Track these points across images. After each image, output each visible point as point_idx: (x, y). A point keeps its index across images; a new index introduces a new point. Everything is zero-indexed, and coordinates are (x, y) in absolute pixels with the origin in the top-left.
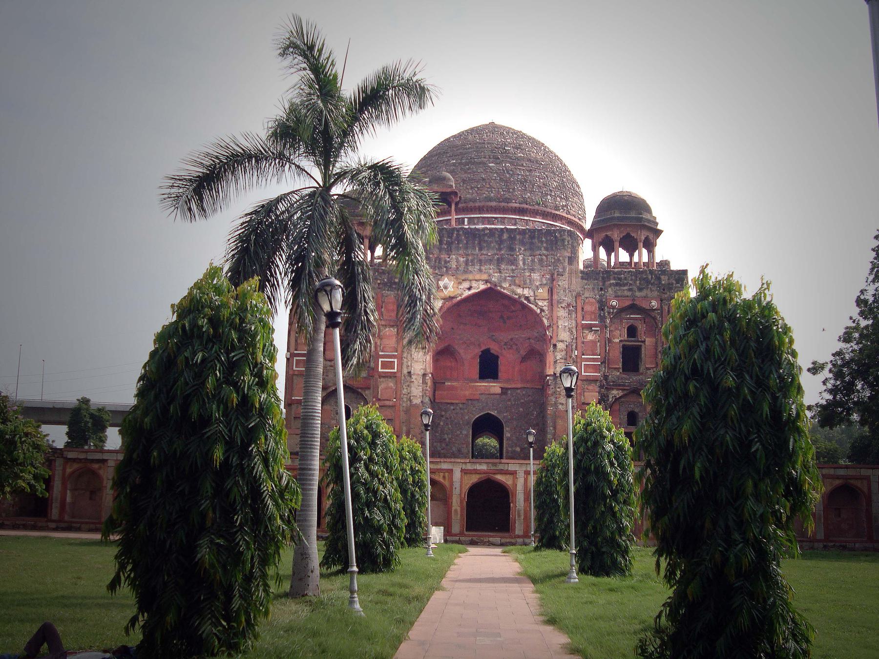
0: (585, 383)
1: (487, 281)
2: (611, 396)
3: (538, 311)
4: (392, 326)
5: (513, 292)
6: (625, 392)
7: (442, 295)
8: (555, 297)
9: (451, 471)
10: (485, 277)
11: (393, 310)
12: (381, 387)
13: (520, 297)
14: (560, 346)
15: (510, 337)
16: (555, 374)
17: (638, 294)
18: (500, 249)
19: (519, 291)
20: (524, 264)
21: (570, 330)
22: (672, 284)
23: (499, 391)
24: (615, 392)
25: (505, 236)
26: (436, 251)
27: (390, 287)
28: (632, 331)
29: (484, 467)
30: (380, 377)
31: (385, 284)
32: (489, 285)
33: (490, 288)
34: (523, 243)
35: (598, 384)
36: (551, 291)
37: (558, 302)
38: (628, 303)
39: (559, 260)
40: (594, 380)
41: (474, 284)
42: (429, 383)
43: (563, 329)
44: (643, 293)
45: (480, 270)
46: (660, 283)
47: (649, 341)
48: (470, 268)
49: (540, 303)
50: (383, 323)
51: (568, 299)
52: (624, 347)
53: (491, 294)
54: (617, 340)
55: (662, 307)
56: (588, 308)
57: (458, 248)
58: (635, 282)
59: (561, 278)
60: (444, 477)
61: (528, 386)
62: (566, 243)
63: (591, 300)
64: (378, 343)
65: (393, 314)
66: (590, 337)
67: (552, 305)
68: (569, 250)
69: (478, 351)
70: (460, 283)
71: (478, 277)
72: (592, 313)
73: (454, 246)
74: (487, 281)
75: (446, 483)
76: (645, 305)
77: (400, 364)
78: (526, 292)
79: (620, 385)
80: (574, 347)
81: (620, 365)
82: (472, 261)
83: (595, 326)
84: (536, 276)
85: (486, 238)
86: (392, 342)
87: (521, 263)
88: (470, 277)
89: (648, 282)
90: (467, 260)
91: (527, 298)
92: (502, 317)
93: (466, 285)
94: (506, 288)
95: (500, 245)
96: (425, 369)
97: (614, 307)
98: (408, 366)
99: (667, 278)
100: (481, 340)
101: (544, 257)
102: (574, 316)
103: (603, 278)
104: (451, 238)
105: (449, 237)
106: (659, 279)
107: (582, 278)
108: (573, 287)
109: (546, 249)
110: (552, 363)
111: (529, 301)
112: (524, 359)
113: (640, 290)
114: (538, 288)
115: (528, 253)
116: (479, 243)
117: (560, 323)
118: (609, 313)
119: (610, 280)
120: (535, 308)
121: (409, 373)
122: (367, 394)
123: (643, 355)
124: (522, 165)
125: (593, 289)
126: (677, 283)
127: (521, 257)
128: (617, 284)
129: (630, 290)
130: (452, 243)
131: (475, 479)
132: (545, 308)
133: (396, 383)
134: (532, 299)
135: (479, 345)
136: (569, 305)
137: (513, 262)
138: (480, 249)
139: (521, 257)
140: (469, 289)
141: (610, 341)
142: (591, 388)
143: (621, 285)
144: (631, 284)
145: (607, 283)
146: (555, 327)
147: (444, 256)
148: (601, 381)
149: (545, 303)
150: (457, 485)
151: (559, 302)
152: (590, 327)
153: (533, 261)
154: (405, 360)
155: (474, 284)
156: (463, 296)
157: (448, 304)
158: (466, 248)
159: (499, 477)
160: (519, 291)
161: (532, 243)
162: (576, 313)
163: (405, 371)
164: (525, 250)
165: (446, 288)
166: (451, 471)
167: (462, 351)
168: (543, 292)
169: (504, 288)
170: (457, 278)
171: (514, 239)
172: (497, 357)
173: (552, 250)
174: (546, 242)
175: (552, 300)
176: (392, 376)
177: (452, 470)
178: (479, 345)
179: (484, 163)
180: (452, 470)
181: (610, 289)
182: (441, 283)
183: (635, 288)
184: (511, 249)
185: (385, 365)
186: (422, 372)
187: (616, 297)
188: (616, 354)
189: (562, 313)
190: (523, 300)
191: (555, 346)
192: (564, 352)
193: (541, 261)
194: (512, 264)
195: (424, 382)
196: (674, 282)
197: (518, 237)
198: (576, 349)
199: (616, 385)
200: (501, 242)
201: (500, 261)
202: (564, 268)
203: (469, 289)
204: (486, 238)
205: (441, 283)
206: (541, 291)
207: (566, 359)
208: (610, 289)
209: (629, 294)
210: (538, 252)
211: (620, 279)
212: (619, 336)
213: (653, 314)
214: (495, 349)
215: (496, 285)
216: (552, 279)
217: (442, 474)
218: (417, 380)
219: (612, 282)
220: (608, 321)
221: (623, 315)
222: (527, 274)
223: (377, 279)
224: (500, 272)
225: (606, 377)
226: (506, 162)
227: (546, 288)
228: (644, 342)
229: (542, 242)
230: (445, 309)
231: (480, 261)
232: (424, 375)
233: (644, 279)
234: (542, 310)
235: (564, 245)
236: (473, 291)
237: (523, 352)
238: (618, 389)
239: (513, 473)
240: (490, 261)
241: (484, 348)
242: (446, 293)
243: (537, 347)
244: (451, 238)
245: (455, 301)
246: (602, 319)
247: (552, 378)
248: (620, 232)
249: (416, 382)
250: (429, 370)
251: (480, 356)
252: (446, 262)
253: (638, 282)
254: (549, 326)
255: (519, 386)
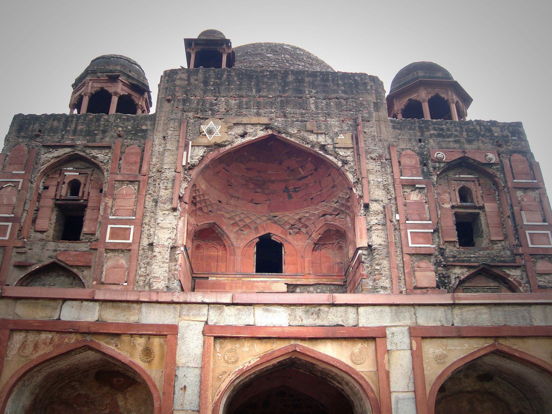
0: (414, 258)
1: (267, 127)
2: (453, 277)
3: (340, 164)
4: (132, 182)
5: (304, 139)
6: (472, 271)
7: (203, 141)
8: (362, 144)
9: (169, 333)
10: (265, 120)
11: (136, 163)
12: (109, 264)
13: (313, 146)
14: (374, 207)
15: (297, 217)
16: (370, 246)
17: (467, 146)
18: (284, 91)
19: (312, 138)
20: (317, 108)
21: (386, 188)
22: (507, 136)
23: (284, 288)
24: (457, 271)
25: (291, 78)
26: (199, 93)
27: (135, 135)
28: (464, 194)
29: (278, 319)
30: (108, 250)
31: (128, 132)
32: (270, 132)
33: (272, 135)
34: (313, 85)
35: (433, 259)
36: (356, 139)
37: (366, 152)
38: (457, 156)
39: (361, 104)
40: (428, 255)
41: (249, 130)
42: (181, 257)
43: (375, 186)
44: (475, 145)
45: (258, 114)
46: (492, 135)
47: (490, 207)
48: (244, 112)
49: (341, 153)
50: (119, 178)
51: (379, 150)
52: (456, 214)
53: (271, 149)
54: (448, 206)
55: (501, 161)
56: (406, 161)
57: (228, 90)
58: (461, 134)
59: (367, 124)
60: (148, 352)
61: (324, 281)
62: (369, 88)
63: (409, 151)
64: (110, 204)
65: (136, 168)
66: (414, 197)
67: (358, 154)
68: (374, 96)
69: (254, 236)
70: (230, 128)
71: (255, 120)
72: (414, 167)
73: (222, 88)
74: (267, 127)
75: (153, 372)
76: (480, 158)
77: (139, 234)
78: (322, 139)
79: (463, 261)
80: (393, 209)
81: (456, 239)
82: (247, 103)
83: (419, 182)
84: (333, 122)
85: (266, 80)
86: (129, 203)
87: (313, 107)
88: (245, 120)
89: (477, 134)
90: (241, 102)
91: (323, 147)
92: (286, 190)
93: (239, 130)
94: (293, 135)
95: (284, 87)
96: (175, 240)
97: (440, 161)
98: (149, 235)
99: (498, 129)
100: (258, 221)
101: (344, 102)
102: (389, 170)
103: (420, 128)
104: (220, 79)
105: (217, 78)
106: (490, 130)
107: (394, 127)
108: (384, 136)
109: (344, 92)
110: (364, 231)
111: (326, 151)
112: (317, 245)
113: (470, 142)
114: (337, 134)
115: (321, 96)
116: (257, 84)
117: (371, 177)
118: (435, 168)
119: (429, 130)
120: (335, 160)
121: (151, 245)
122: (85, 275)
123: (484, 226)
124: (302, 59)
125: (410, 140)
126: (513, 133)
127: (312, 101)
128: (439, 135)
129: (456, 142)
130: (221, 84)
131: (250, 356)
132: (348, 158)
133: (130, 260)
134: (330, 147)
135: (256, 228)
136: (380, 157)
137: (303, 105)
138: (259, 91)
139: (312, 101)
140: (243, 136)
141: (438, 205)
142: (423, 264)
143: (444, 137)
144: (456, 136)
145: (427, 134)
146: (365, 182)
147: (210, 98)
148: (436, 256)
149: (349, 153)
150: (188, 378)
151: (367, 152)
152: (412, 185)
153: (328, 105)
154: (147, 227)
155: (249, 130)
156: (235, 145)
157: (213, 155)
158: (240, 89)
159: (330, 351)
160: (312, 138)
161: (326, 86)
162: (392, 166)
163: (145, 242)
164: (317, 93)
165: (210, 132)
166: (169, 333)
167: (232, 236)
168: (345, 139)
169: (291, 135)
170: (226, 122)
171: (302, 81)
172: (280, 246)
173: (353, 94)
174: (344, 85)
175: (358, 149)
176: (125, 250)
177: (173, 329)
178: (256, 228)
179: (261, 54)
180: (173, 329)
181: (431, 140)
182: (204, 128)
183: (463, 140)
184: (299, 91)
185: (115, 234)
186: (170, 243)
187: (441, 148)
188: (449, 223)
189: (372, 166)
190: (317, 149)
191: (367, 206)
192: (380, 217)
193: (339, 105)
194: (301, 107)
195: (173, 259)
196: (509, 134)
197: (307, 79)
198: (397, 212)
199: (458, 261)
200: (285, 84)
201: (283, 105)
202: (370, 113)
203: (243, 136)
204: (266, 80)
205: (204, 128)
206: (341, 136)
207: (383, 225)
208: (431, 140)
209: (457, 146)
210: (334, 95)
211: (442, 130)
212: (449, 200)
213: (491, 171)
214: (277, 234)
215: (279, 132)
216: (356, 125)
217: (141, 341)
218: (162, 254)
219: (432, 132)
220: (435, 178)
221: (451, 174)
222: (321, 118)
223: (118, 126)
224: (285, 116)
225: (442, 251)
226: (285, 54)
227: (349, 135)
228: (482, 208)
229: (338, 85)
230: (207, 161)
231: (258, 103)
232: (173, 248)
233: (471, 131)
234: (345, 163)
235: (367, 90)
236: (248, 139)
237: (316, 236)
238: (461, 267)
239: (373, 337)
240: (272, 104)
241: (262, 233)
242: (210, 139)
243: (338, 222)
244: (220, 79)
245: (222, 150)
246: (427, 175)
247: (365, 252)
248: (428, 93)
249: (159, 257)
250: (182, 240)
251: (258, 245)
252: (212, 104)
253: (465, 133)
254: (358, 181)
255: (312, 281)
